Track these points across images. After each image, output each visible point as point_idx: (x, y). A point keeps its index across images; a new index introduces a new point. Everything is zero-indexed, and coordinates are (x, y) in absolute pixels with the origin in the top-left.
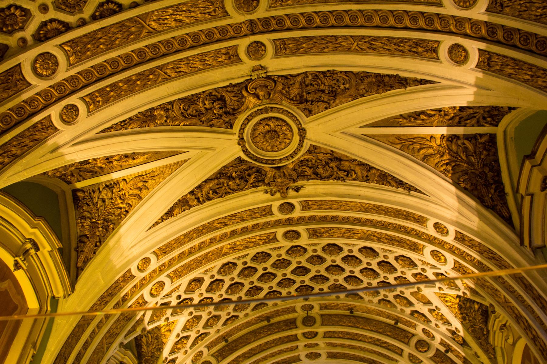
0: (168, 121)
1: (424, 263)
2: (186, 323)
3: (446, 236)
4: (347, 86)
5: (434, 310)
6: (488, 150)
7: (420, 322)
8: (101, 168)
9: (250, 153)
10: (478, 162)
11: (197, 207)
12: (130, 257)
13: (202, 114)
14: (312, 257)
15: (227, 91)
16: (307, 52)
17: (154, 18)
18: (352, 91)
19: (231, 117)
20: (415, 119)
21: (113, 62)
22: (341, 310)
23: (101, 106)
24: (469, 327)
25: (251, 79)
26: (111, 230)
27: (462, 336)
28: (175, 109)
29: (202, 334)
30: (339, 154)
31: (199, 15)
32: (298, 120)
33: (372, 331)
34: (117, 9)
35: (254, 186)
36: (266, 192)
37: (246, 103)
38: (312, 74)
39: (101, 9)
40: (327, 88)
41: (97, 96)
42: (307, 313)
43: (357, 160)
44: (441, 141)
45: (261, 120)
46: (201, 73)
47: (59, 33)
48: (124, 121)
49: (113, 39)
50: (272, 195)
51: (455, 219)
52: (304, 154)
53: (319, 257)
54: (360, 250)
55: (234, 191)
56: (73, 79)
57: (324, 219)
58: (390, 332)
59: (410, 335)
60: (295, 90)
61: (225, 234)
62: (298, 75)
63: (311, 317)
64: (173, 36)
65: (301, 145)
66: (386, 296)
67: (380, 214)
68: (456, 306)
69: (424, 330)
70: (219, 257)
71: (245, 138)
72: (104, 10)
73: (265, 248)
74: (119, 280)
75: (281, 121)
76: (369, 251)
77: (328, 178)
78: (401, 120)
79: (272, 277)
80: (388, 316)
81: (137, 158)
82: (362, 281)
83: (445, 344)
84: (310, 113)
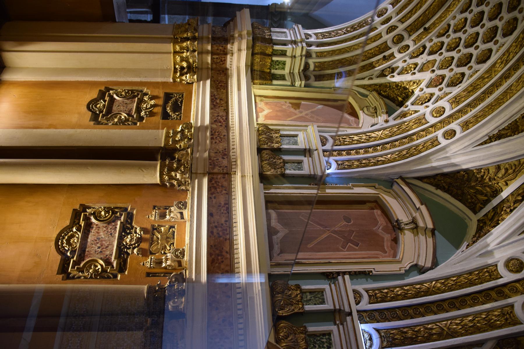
3: (443, 134)
6: (470, 203)
7: (415, 49)
10: (468, 192)
24: (391, 85)
33: (431, 5)
44: (499, 186)
51: (448, 149)
67: (495, 100)
68: (408, 87)
69: (408, 47)
83: (390, 58)
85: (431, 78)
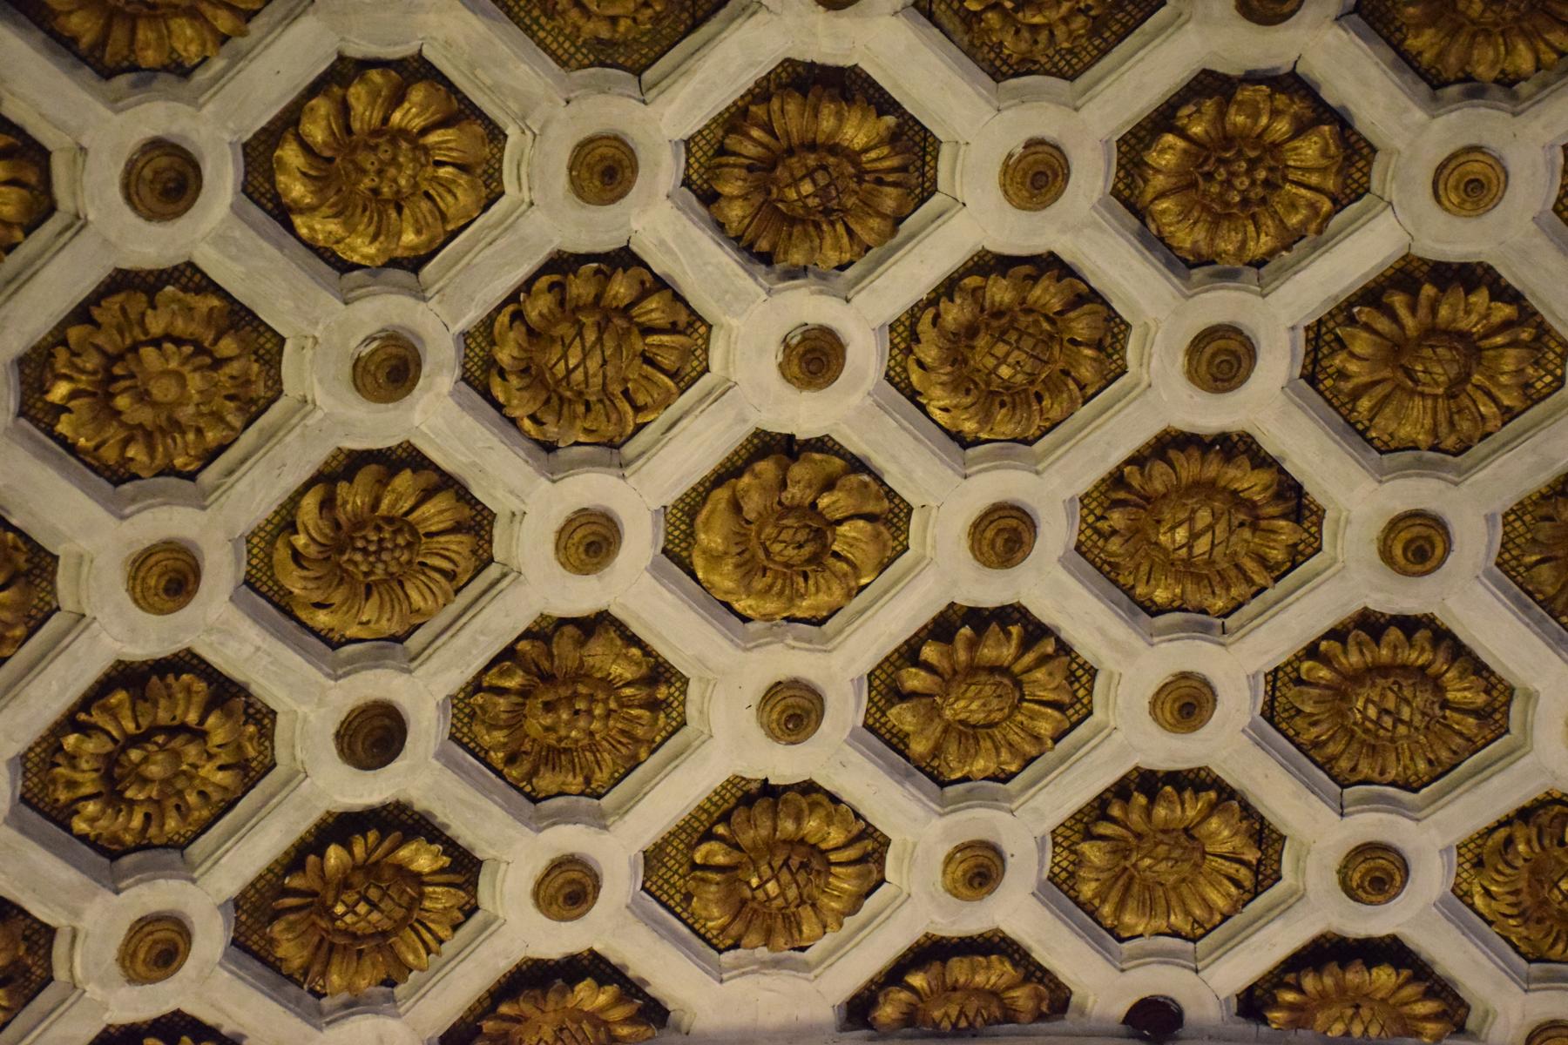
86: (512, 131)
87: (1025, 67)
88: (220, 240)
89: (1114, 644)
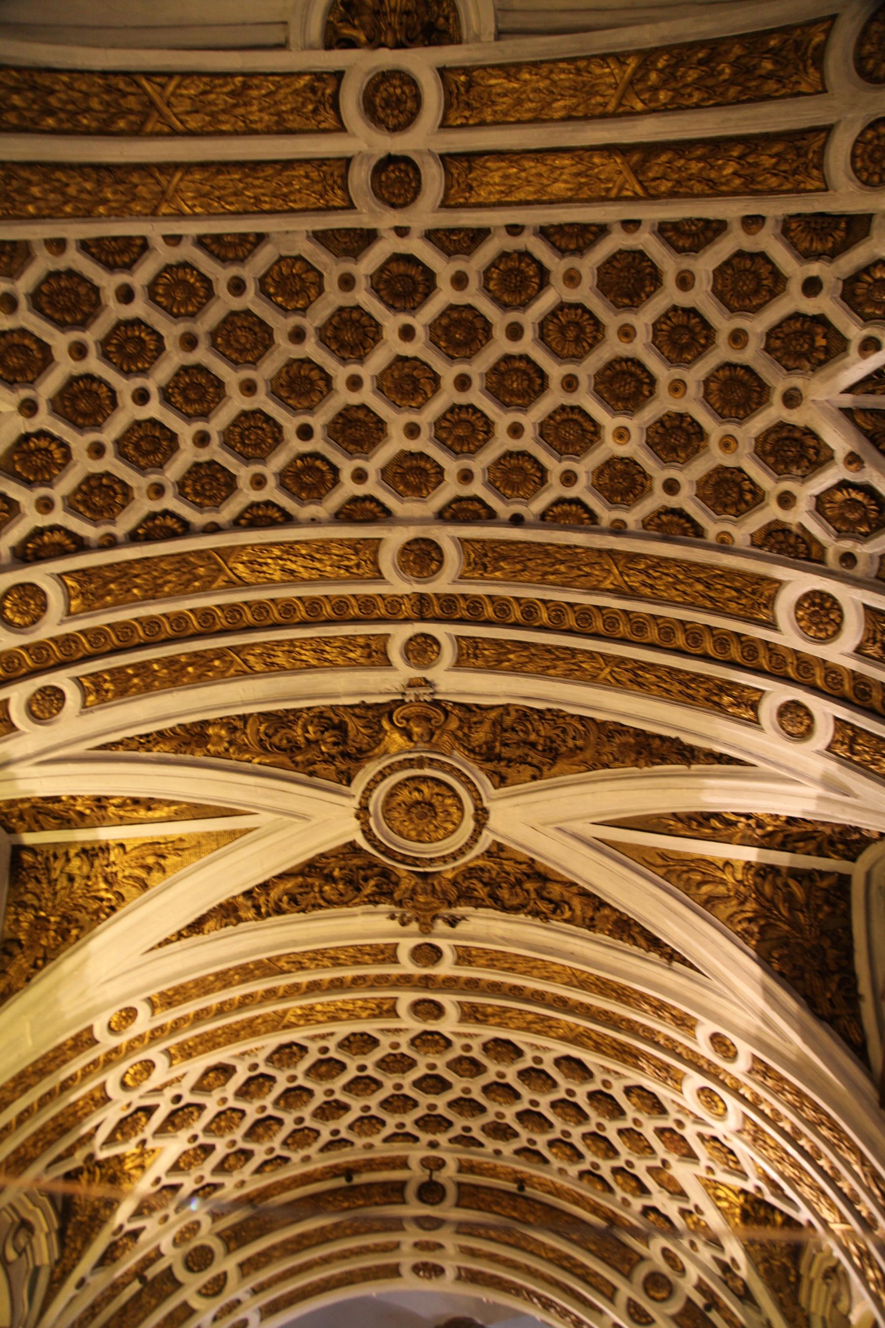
0: (231, 750)
1: (681, 1109)
2: (180, 1157)
4: (580, 743)
5: (690, 1212)
8: (81, 814)
9: (375, 836)
11: (253, 923)
12: (99, 1001)
13: (299, 748)
14: (460, 1060)
15: (354, 715)
16: (516, 670)
17: (245, 558)
18: (588, 754)
19: (353, 765)
20: (700, 824)
21: (152, 622)
22: (499, 1178)
23: (110, 700)
25: (403, 701)
26: (72, 940)
27: (743, 1280)
28: (248, 731)
29: (209, 1185)
30: (546, 867)
31: (328, 569)
32: (477, 790)
34: (180, 530)
35: (370, 902)
36: (392, 917)
37: (384, 743)
38: (517, 711)
39: (150, 524)
40: (541, 741)
41: (105, 681)
42: (431, 1176)
43: (576, 884)
45: (408, 779)
46: (310, 673)
47: (62, 552)
48: (147, 736)
49: (160, 581)
50: (403, 924)
52: (477, 857)
53: (473, 1062)
54: (558, 1062)
55: (330, 903)
56: (68, 640)
57: (495, 989)
58: (595, 1243)
59: (636, 1257)
60: (482, 734)
61: (296, 987)
62: (492, 708)
63: (436, 1184)
64: (272, 597)
65: (475, 838)
66: (596, 1166)
68: (738, 1211)
69: (665, 1252)
70: (275, 1029)
71: (371, 809)
72: (156, 526)
73: (370, 1027)
74: (64, 1044)
75: (444, 788)
76: (574, 1065)
77: (515, 909)
78: (672, 823)
79: (374, 1086)
80: (595, 1209)
81: (155, 809)
82: (551, 1125)
84: (501, 781)
85: (679, 1161)
86: (325, 274)
87: (457, 252)
88: (253, 302)
89: (497, 414)
